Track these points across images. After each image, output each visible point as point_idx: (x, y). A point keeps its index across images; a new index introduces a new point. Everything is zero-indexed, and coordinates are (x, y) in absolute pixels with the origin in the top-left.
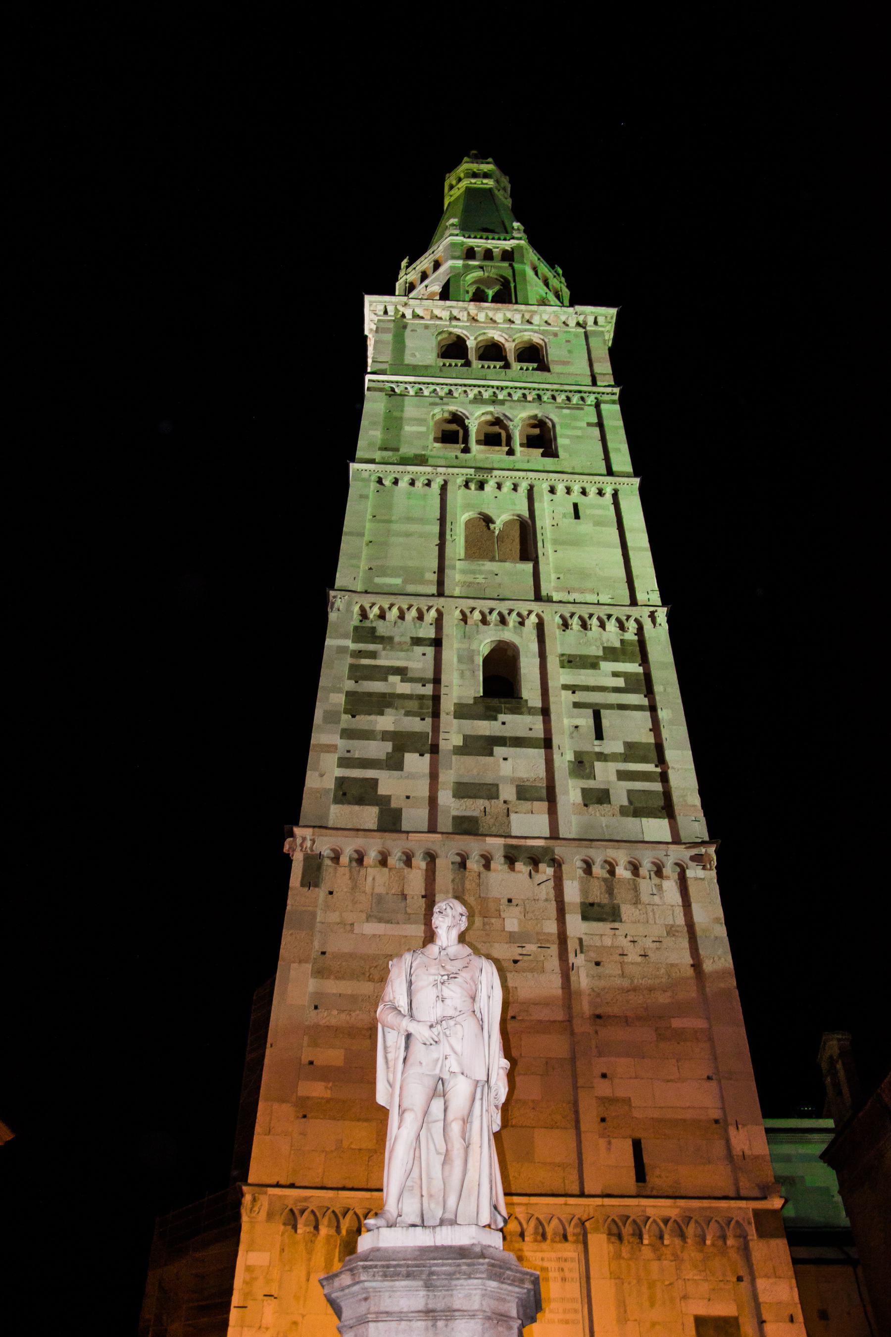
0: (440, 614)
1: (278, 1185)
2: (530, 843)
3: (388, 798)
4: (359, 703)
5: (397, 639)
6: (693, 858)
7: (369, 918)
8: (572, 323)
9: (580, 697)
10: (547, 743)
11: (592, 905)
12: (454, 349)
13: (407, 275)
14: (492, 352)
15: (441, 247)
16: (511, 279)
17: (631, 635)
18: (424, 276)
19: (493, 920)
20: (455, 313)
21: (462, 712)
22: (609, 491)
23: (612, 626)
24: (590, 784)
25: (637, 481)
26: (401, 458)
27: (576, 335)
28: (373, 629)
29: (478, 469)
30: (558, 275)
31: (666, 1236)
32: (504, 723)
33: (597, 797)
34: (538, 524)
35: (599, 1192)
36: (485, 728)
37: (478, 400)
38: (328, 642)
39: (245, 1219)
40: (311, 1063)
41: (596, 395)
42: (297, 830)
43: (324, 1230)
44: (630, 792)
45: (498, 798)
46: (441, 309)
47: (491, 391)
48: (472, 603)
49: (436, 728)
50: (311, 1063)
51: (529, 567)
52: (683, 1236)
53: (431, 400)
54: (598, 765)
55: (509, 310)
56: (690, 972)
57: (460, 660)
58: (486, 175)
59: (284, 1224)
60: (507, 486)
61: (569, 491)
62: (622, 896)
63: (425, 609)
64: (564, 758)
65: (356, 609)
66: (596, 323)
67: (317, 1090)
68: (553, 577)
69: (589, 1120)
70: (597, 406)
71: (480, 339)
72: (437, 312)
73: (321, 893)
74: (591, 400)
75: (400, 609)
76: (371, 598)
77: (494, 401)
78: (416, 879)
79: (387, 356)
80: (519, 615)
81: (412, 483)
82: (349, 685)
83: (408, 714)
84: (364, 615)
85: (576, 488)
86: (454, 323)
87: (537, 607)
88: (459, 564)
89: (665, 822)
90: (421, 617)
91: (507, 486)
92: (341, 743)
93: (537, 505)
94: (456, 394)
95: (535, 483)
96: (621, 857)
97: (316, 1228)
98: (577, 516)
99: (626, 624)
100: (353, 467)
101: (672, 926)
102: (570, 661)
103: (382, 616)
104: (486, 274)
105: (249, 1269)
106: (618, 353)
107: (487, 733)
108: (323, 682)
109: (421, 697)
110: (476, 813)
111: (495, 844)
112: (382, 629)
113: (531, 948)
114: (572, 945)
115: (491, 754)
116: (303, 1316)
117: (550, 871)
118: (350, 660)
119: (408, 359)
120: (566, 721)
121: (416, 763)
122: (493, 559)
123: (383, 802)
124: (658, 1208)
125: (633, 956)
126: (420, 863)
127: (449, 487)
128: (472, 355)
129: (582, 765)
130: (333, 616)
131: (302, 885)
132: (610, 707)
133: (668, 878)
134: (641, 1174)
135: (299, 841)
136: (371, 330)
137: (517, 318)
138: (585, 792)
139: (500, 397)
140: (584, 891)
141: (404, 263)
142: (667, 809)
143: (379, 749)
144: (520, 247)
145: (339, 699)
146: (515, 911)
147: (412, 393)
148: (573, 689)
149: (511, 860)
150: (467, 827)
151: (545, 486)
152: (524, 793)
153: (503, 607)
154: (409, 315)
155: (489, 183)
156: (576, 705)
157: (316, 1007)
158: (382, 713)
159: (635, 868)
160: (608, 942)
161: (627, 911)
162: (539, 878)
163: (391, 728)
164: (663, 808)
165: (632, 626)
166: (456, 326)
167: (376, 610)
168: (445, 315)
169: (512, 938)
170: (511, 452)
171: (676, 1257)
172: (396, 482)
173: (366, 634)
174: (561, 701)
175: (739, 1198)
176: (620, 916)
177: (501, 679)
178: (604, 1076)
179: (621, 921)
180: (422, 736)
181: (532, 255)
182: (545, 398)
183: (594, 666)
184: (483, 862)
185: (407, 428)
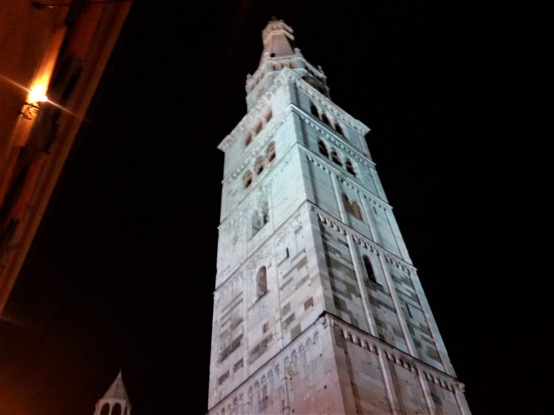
5: (333, 236)
12: (314, 111)
14: (325, 120)
27: (355, 132)
33: (417, 344)
37: (329, 140)
44: (428, 347)
77: (335, 145)
83: (347, 274)
109: (350, 269)
113: (420, 408)
115: (379, 307)
123: (350, 313)
129: (410, 327)
142: (439, 359)
158: (338, 270)
163: (343, 279)
183: (400, 283)
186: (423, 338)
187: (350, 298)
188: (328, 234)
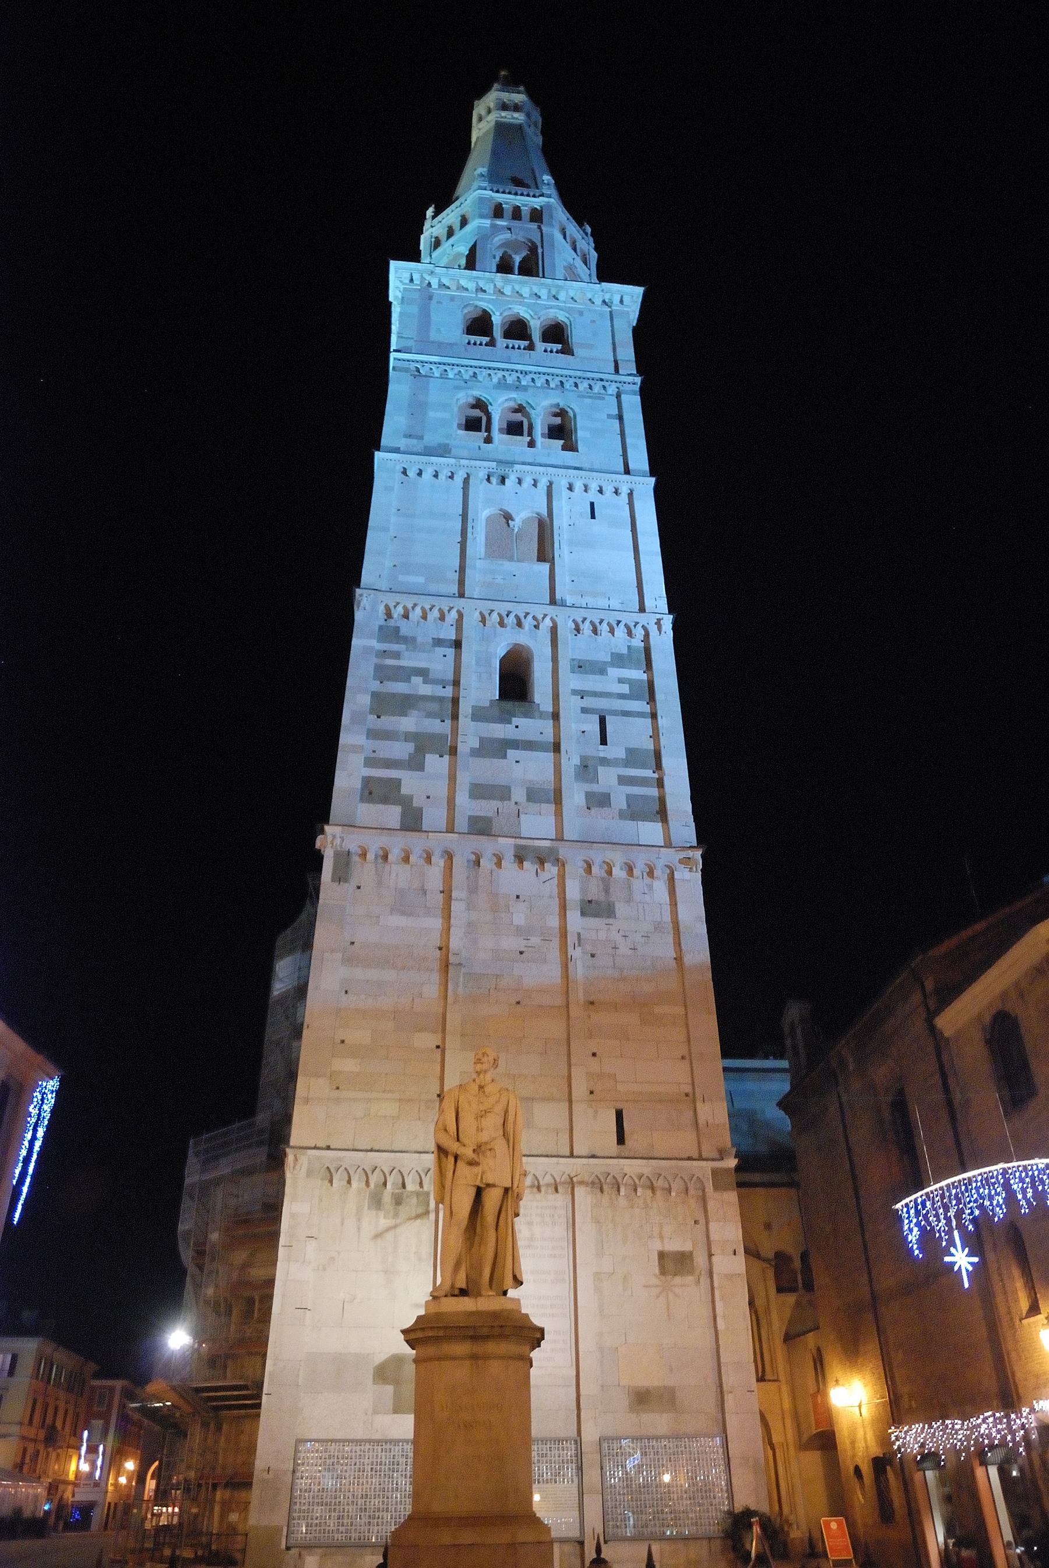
0: (461, 615)
1: (315, 1148)
2: (537, 843)
3: (411, 798)
4: (382, 704)
5: (419, 640)
6: (681, 861)
7: (393, 910)
8: (598, 301)
9: (590, 702)
10: (557, 748)
11: (590, 902)
12: (479, 325)
13: (433, 227)
14: (517, 330)
15: (468, 201)
16: (539, 244)
17: (637, 642)
18: (450, 233)
19: (503, 915)
20: (482, 284)
21: (479, 715)
22: (624, 491)
23: (620, 632)
24: (595, 788)
25: (653, 480)
26: (425, 447)
27: (601, 315)
28: (397, 629)
29: (500, 462)
30: (586, 234)
31: (639, 1190)
32: (517, 727)
34: (556, 523)
35: (584, 1154)
36: (499, 731)
37: (502, 385)
38: (355, 642)
39: (288, 1175)
40: (343, 1042)
41: (618, 385)
42: (326, 827)
43: (355, 1184)
44: (628, 797)
45: (509, 799)
46: (468, 279)
47: (515, 375)
48: (490, 605)
49: (455, 731)
50: (343, 1042)
51: (546, 567)
52: (653, 1189)
53: (456, 383)
54: (600, 769)
55: (535, 284)
56: (673, 963)
57: (477, 664)
58: (517, 108)
59: (322, 1179)
60: (528, 481)
61: (586, 489)
62: (617, 894)
63: (446, 609)
64: (570, 761)
65: (381, 608)
66: (621, 302)
67: (348, 1065)
68: (568, 579)
69: (580, 1090)
70: (618, 396)
71: (505, 314)
72: (463, 282)
73: (348, 888)
74: (612, 389)
75: (423, 609)
76: (398, 598)
78: (434, 875)
79: (412, 333)
80: (534, 618)
81: (436, 476)
82: (375, 686)
83: (430, 715)
84: (389, 615)
85: (594, 487)
86: (481, 295)
87: (551, 610)
88: (479, 564)
89: (659, 826)
90: (442, 618)
91: (528, 481)
92: (369, 745)
93: (555, 503)
94: (480, 378)
95: (554, 479)
96: (617, 858)
97: (349, 1182)
98: (593, 516)
99: (634, 631)
100: (378, 455)
101: (660, 923)
102: (581, 667)
103: (406, 616)
104: (514, 237)
105: (293, 1216)
106: (644, 334)
107: (502, 737)
108: (350, 682)
109: (441, 700)
110: (490, 814)
111: (506, 845)
112: (406, 628)
113: (535, 940)
114: (571, 939)
116: (339, 1253)
117: (555, 870)
118: (375, 660)
119: (434, 336)
120: (574, 726)
121: (436, 764)
122: (511, 559)
123: (406, 803)
124: (632, 1167)
125: (624, 949)
126: (439, 862)
127: (471, 481)
128: (498, 332)
129: (586, 769)
130: (359, 615)
131: (333, 881)
132: (615, 713)
133: (658, 878)
134: (621, 1139)
135: (329, 838)
136: (396, 297)
137: (544, 293)
138: (589, 796)
139: (524, 383)
140: (584, 890)
141: (430, 212)
142: (662, 814)
143: (402, 750)
144: (549, 206)
145: (366, 700)
146: (522, 906)
147: (437, 374)
148: (582, 694)
149: (520, 859)
150: (481, 827)
151: (564, 483)
152: (533, 795)
153: (520, 610)
154: (435, 284)
155: (519, 117)
156: (584, 710)
157: (346, 992)
158: (404, 714)
159: (630, 869)
160: (602, 935)
161: (620, 908)
162: (544, 876)
164: (658, 813)
165: (639, 633)
166: (481, 300)
167: (400, 610)
168: (471, 286)
169: (519, 931)
170: (531, 444)
171: (646, 1206)
172: (420, 474)
173: (390, 633)
174: (570, 705)
175: (701, 1158)
176: (614, 912)
177: (515, 682)
178: (594, 1055)
179: (615, 917)
180: (442, 737)
181: (561, 215)
182: (567, 385)
183: (602, 672)
184: (495, 860)
185: (432, 414)
186: (623, 780)
187: (421, 767)
188: (405, 640)
